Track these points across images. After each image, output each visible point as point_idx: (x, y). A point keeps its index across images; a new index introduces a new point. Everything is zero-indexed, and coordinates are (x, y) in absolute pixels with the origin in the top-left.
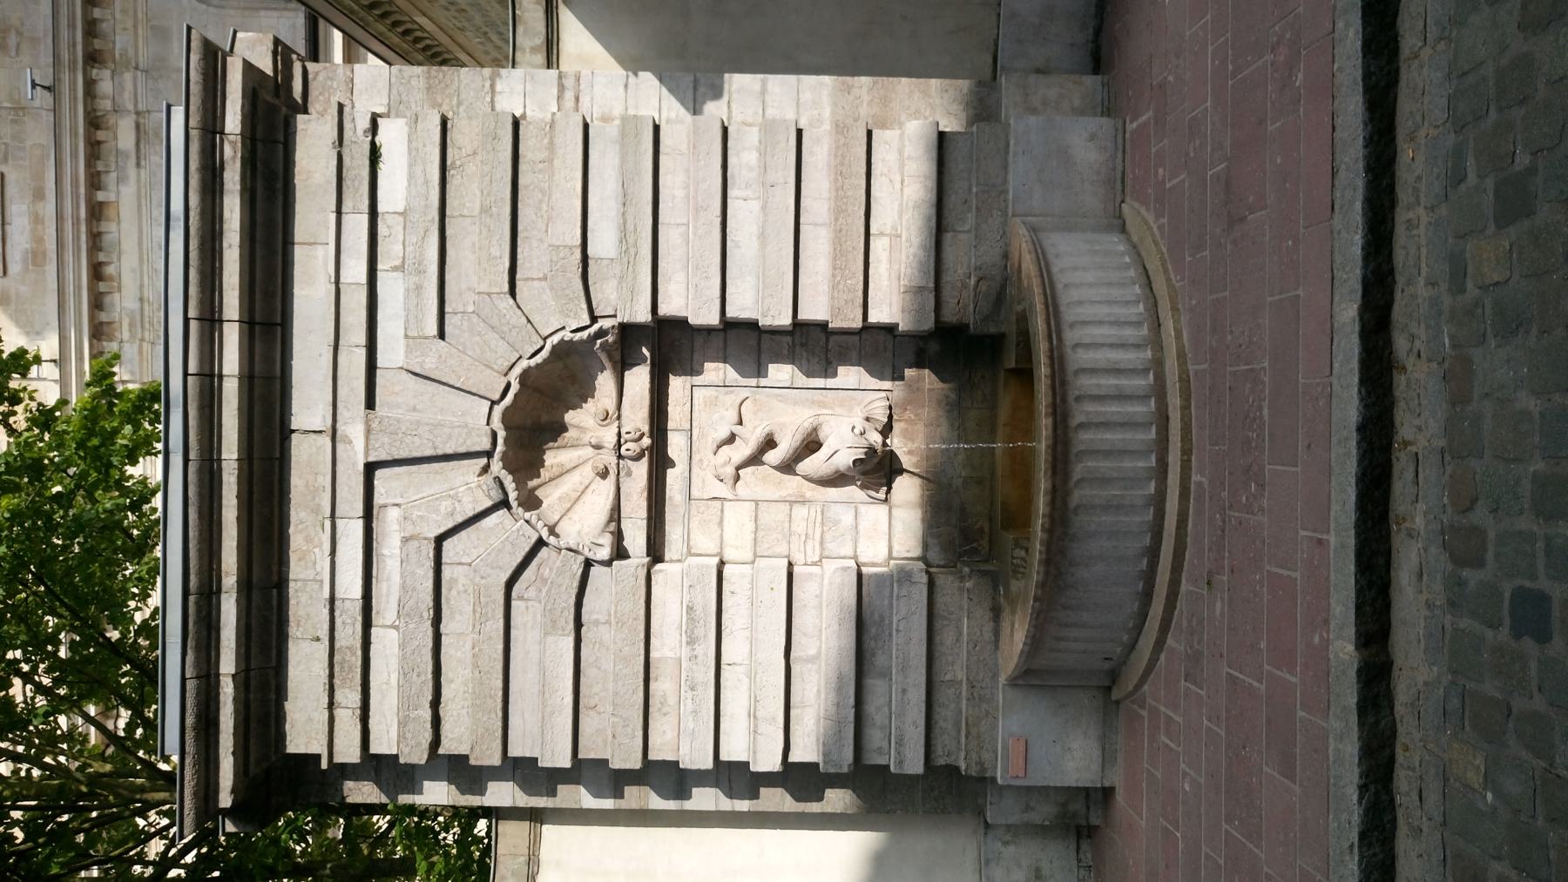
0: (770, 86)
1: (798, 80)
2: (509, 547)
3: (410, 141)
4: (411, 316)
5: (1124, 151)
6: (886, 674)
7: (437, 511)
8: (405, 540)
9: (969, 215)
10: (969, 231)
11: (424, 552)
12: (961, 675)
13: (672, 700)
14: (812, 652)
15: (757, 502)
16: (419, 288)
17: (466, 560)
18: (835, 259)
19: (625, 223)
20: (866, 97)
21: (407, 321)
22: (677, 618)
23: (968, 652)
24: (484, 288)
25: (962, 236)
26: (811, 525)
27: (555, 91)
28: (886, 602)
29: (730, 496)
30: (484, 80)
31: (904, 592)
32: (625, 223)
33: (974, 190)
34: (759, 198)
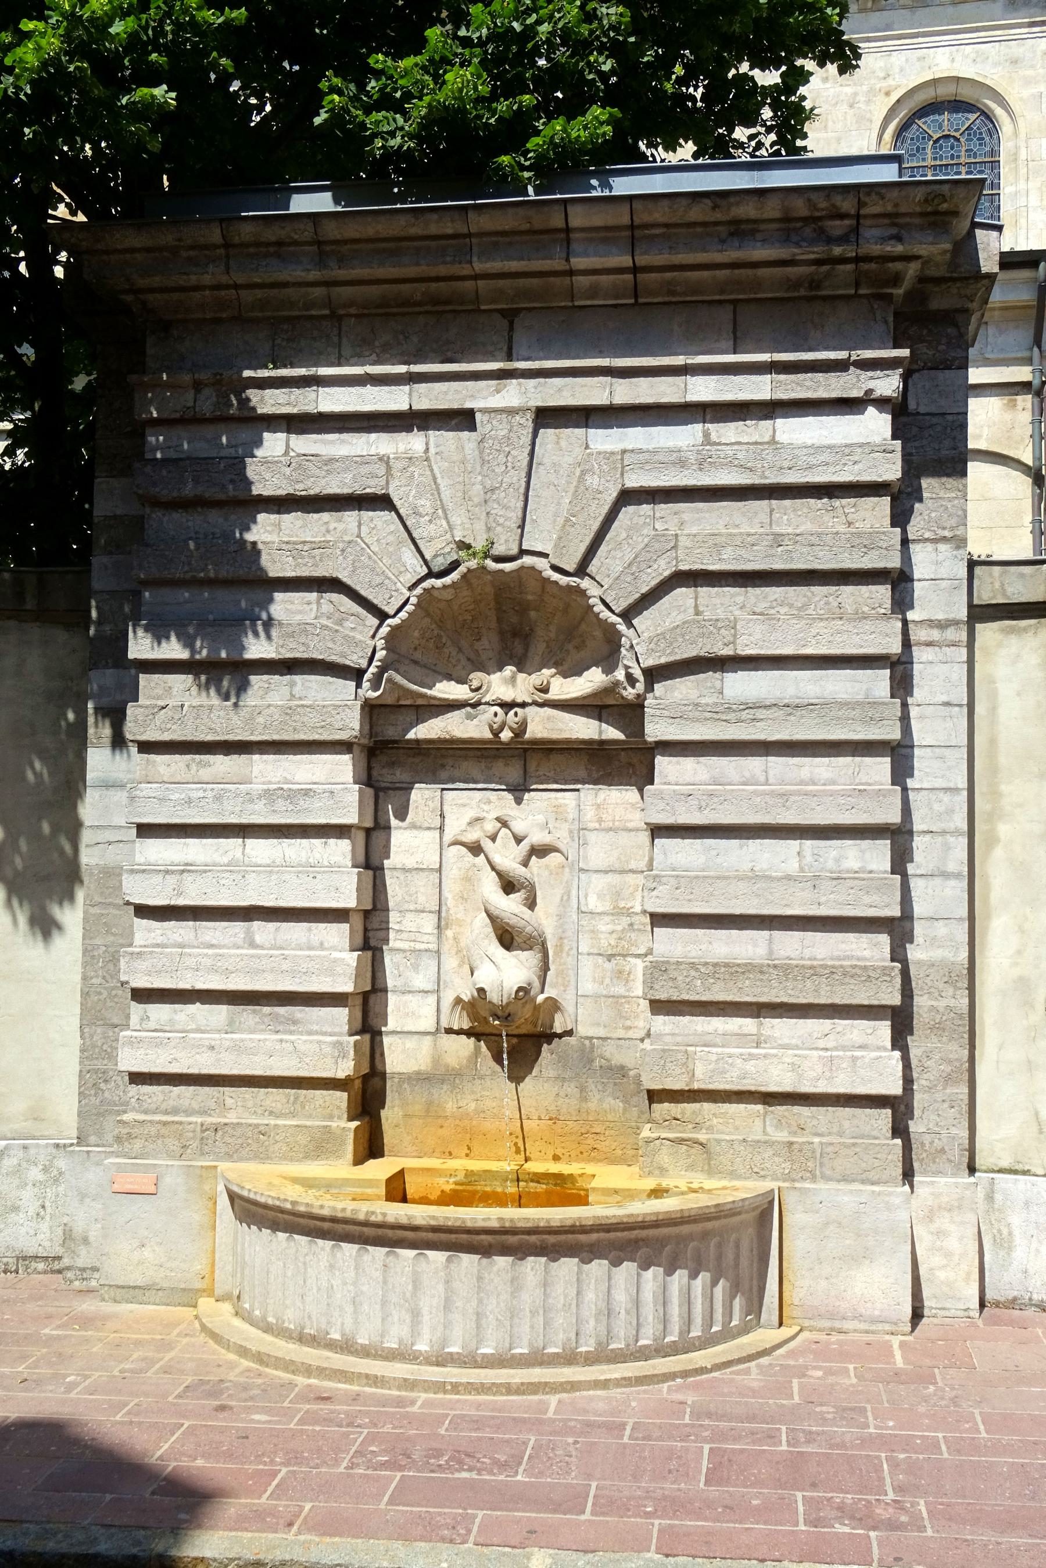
0: (953, 883)
1: (961, 919)
2: (378, 580)
3: (861, 445)
4: (651, 458)
5: (867, 1332)
6: (231, 1027)
7: (419, 495)
8: (385, 460)
9: (786, 1134)
10: (765, 1133)
11: (372, 482)
12: (232, 1118)
13: (205, 774)
14: (258, 939)
15: (440, 870)
16: (682, 463)
17: (364, 529)
18: (727, 965)
19: (766, 707)
20: (941, 1004)
21: (641, 451)
22: (297, 778)
23: (257, 1126)
24: (683, 541)
25: (758, 1123)
26: (412, 936)
27: (941, 616)
28: (315, 1027)
29: (448, 838)
30: (952, 529)
31: (327, 1050)
32: (766, 707)
33: (816, 1140)
34: (802, 870)
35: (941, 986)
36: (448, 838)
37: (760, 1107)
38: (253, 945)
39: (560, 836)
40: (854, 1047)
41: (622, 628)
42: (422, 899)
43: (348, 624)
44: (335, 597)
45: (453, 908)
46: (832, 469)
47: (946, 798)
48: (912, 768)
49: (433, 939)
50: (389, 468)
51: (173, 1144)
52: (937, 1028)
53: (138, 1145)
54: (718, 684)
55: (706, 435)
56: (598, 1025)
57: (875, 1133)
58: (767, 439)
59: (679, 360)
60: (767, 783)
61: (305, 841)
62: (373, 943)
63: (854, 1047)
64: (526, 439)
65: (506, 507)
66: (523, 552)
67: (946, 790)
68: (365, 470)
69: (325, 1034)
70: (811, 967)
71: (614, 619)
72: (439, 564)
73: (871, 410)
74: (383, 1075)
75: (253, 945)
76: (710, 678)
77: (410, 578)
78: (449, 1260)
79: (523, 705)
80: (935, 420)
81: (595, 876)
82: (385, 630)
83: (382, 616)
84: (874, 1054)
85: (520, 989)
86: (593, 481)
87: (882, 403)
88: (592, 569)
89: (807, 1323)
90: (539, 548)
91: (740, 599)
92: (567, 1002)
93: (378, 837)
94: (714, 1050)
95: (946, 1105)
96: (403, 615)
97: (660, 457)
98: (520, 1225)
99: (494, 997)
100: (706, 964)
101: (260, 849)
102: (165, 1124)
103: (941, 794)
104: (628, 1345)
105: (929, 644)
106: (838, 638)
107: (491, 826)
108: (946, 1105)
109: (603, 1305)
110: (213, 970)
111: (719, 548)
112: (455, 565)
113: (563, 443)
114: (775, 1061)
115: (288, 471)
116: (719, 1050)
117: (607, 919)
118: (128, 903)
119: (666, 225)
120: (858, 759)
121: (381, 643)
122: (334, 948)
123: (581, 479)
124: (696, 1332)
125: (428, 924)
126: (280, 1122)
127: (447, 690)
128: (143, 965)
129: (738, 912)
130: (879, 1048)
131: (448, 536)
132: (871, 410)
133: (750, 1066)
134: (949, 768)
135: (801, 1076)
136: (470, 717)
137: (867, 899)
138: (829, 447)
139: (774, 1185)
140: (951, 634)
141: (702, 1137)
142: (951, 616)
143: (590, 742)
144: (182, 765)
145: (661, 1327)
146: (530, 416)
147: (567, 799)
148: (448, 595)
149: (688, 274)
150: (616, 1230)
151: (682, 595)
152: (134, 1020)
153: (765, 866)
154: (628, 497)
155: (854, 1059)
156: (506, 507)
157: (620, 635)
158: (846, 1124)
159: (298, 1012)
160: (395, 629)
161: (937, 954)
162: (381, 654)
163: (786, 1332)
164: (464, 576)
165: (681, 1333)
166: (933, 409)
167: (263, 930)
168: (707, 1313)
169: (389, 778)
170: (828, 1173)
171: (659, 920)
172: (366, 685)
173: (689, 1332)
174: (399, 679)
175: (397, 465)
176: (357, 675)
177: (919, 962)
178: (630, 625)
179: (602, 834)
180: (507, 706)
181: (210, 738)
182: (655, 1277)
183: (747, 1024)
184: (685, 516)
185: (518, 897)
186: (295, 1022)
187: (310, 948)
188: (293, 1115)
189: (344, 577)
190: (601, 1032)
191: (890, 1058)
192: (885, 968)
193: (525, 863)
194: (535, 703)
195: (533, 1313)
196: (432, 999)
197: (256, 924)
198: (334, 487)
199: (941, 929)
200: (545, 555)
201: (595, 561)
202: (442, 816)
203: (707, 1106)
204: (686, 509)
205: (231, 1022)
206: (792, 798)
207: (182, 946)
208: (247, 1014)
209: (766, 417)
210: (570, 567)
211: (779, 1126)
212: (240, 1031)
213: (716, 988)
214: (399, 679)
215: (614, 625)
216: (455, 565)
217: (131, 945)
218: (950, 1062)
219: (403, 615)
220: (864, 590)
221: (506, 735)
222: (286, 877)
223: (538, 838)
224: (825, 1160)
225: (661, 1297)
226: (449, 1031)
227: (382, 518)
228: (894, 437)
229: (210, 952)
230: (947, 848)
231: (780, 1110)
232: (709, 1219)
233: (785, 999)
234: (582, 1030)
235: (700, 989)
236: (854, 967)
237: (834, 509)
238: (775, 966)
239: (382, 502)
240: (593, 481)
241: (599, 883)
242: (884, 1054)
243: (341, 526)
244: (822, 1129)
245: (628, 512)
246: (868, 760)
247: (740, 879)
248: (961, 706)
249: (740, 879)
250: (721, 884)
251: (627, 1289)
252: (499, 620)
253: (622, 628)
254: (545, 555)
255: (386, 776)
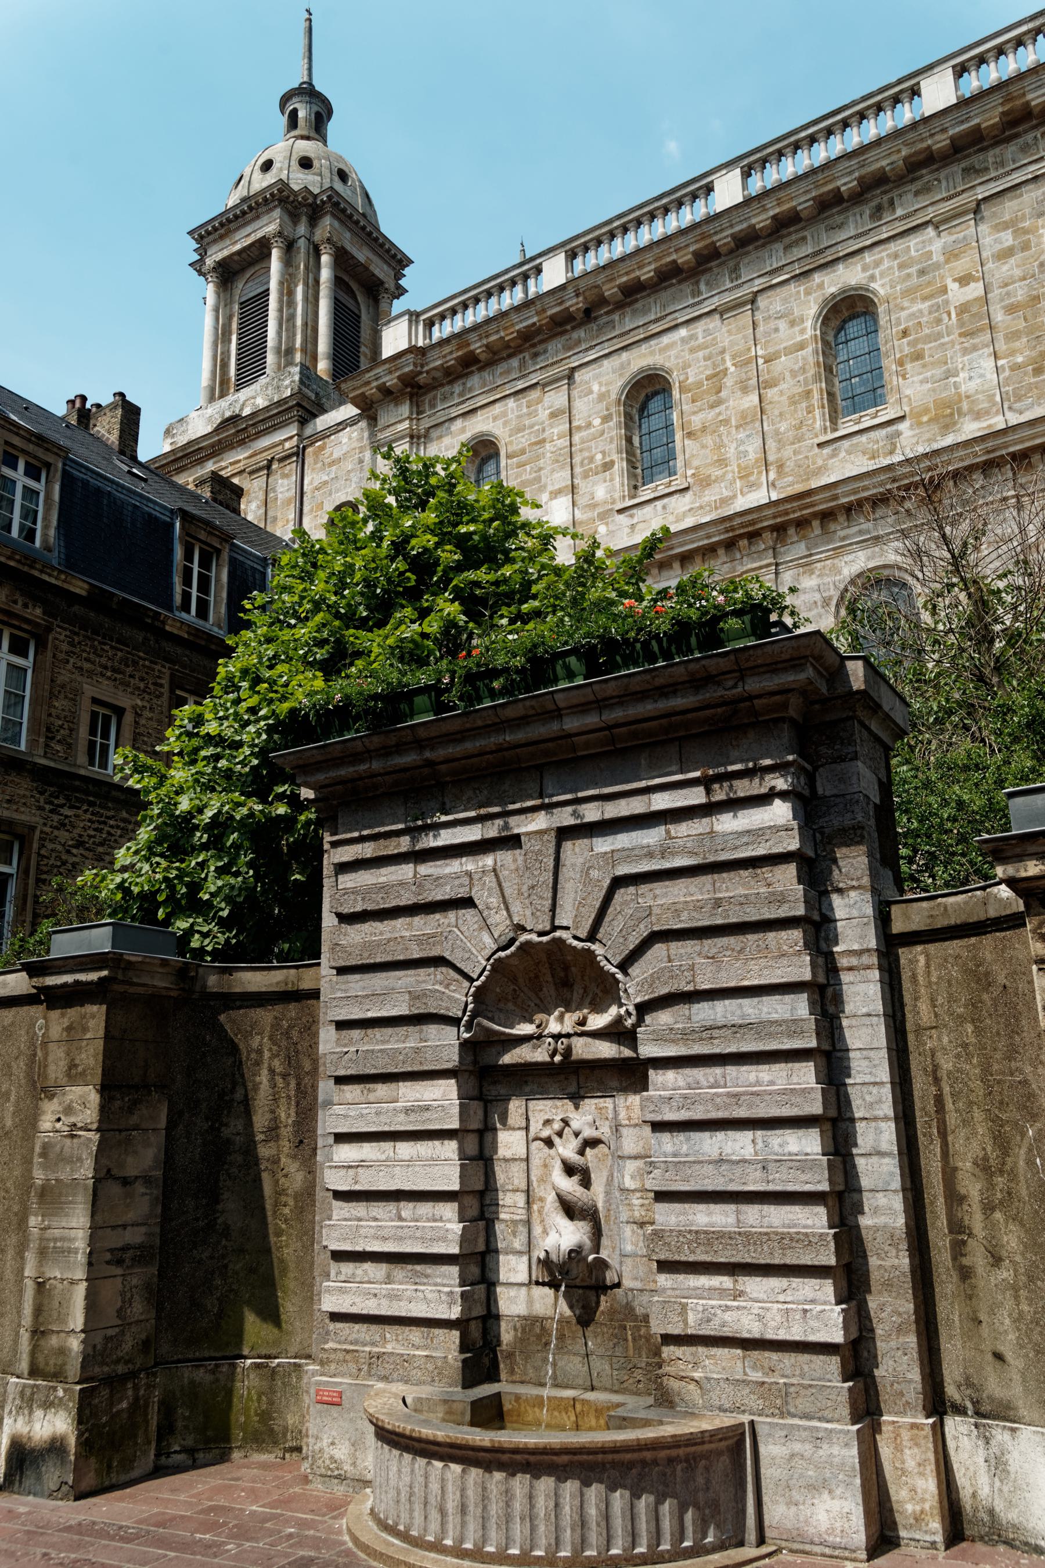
0: (886, 1160)
2: (467, 955)
3: (770, 827)
4: (628, 855)
5: (831, 1557)
6: (389, 1279)
7: (490, 896)
8: (469, 874)
9: (760, 1374)
10: (745, 1374)
11: (462, 890)
12: (389, 1348)
13: (372, 1097)
14: (403, 1214)
15: (527, 1159)
16: (650, 855)
17: (460, 922)
18: (706, 1232)
19: (719, 1028)
20: (887, 1263)
21: (624, 850)
22: (425, 1097)
23: (402, 1355)
24: (656, 911)
25: (739, 1364)
26: (512, 1210)
27: (856, 947)
28: (439, 1280)
29: (532, 1135)
30: (858, 879)
31: (444, 1297)
32: (719, 1028)
33: (782, 1381)
34: (756, 1154)
35: (887, 1248)
36: (532, 1135)
37: (739, 1351)
38: (400, 1219)
39: (604, 1131)
40: (806, 1302)
41: (620, 976)
42: (516, 1182)
43: (452, 987)
44: (444, 969)
45: (538, 1190)
46: (751, 847)
47: (874, 1090)
48: (849, 1068)
49: (524, 1211)
50: (471, 879)
51: (353, 1367)
52: (888, 1285)
53: (333, 1366)
54: (687, 1013)
55: (668, 832)
56: (636, 1279)
57: (828, 1376)
58: (708, 830)
59: (643, 784)
60: (725, 1086)
61: (430, 1143)
62: (487, 1215)
63: (806, 1302)
64: (552, 850)
65: (541, 898)
66: (554, 928)
67: (875, 1084)
68: (457, 882)
69: (444, 1285)
70: (766, 1234)
71: (614, 970)
72: (504, 940)
73: (777, 802)
74: (497, 1317)
75: (400, 1219)
76: (682, 1009)
77: (487, 952)
78: (463, 1471)
79: (568, 1036)
80: (838, 800)
81: (628, 1162)
82: (473, 989)
83: (471, 980)
84: (819, 1308)
85: (571, 1251)
86: (595, 874)
87: (783, 795)
88: (599, 936)
89: (784, 1544)
90: (565, 924)
91: (698, 948)
92: (613, 1261)
93: (488, 1137)
94: (701, 1302)
95: (900, 1353)
96: (483, 978)
97: (636, 852)
98: (506, 1445)
99: (554, 1257)
100: (690, 1231)
101: (405, 1149)
102: (347, 1351)
103: (871, 1087)
104: (599, 1553)
105: (850, 969)
106: (765, 972)
107: (557, 1126)
108: (900, 1353)
109: (577, 1517)
110: (376, 1238)
111: (677, 913)
112: (512, 941)
113: (577, 850)
114: (745, 1312)
115: (414, 888)
116: (704, 1302)
117: (638, 1195)
118: (328, 1190)
119: (618, 697)
120: (790, 1065)
121: (470, 999)
122: (449, 1221)
123: (587, 874)
124: (665, 1546)
125: (520, 1199)
126: (417, 1353)
127: (526, 1029)
128: (335, 1234)
129: (710, 1188)
130: (825, 1303)
131: (508, 922)
132: (777, 802)
133: (728, 1316)
134: (875, 1066)
135: (765, 1325)
136: (536, 1047)
137: (804, 1177)
138: (748, 832)
139: (745, 1418)
140: (866, 959)
141: (697, 1375)
142: (865, 946)
143: (613, 1060)
144: (359, 1091)
145: (630, 1539)
146: (553, 834)
147: (608, 1103)
148: (515, 962)
149: (645, 725)
150: (581, 1453)
151: (659, 950)
152: (333, 1274)
153: (730, 1151)
154: (619, 882)
155: (805, 1311)
156: (541, 898)
157: (617, 981)
158: (806, 1368)
159: (429, 1269)
160: (478, 988)
161: (881, 1220)
162: (470, 1007)
163: (764, 1550)
164: (520, 948)
165: (574, 1551)
166: (835, 792)
167: (407, 1209)
168: (653, 1530)
169: (494, 1093)
170: (792, 1410)
171: (662, 1196)
172: (462, 1029)
173: (658, 1545)
174: (486, 1023)
175: (476, 877)
176: (455, 1022)
177: (867, 1228)
178: (626, 974)
179: (631, 1129)
180: (557, 1037)
181: (373, 1071)
182: (622, 1496)
183: (725, 1281)
184: (658, 892)
185: (576, 1178)
186: (427, 1276)
187: (435, 1220)
188: (426, 1347)
189: (447, 955)
190: (638, 1285)
191: (832, 1310)
192: (821, 1235)
193: (581, 1152)
194: (576, 1034)
195: (522, 1519)
196: (525, 1258)
197: (402, 1204)
198: (439, 895)
199: (881, 1200)
200: (567, 928)
201: (602, 930)
202: (527, 1119)
203: (701, 1350)
204: (659, 888)
205: (388, 1276)
206: (743, 1098)
207: (360, 1220)
208: (400, 1272)
209: (705, 816)
210: (583, 935)
211: (754, 1368)
212: (394, 1282)
213: (698, 1251)
214: (486, 1023)
215: (613, 975)
216: (512, 941)
217: (330, 1219)
218: (900, 1314)
219: (483, 978)
220: (783, 934)
221: (558, 1058)
222: (417, 1169)
223: (588, 1133)
224: (790, 1399)
225: (628, 1513)
226: (537, 1283)
227: (468, 914)
228: (794, 819)
229: (374, 1224)
230: (879, 1132)
231: (755, 1354)
232: (696, 1444)
233: (749, 1260)
234: (627, 1283)
235: (687, 1252)
236: (798, 1233)
237: (757, 875)
238: (740, 1233)
239: (467, 902)
240: (595, 874)
241: (631, 1166)
242: (827, 1307)
243: (446, 921)
244: (788, 1372)
245: (623, 895)
246: (797, 1065)
247: (710, 1162)
248: (878, 1015)
249: (710, 1162)
250: (698, 1167)
251: (597, 1505)
252: (553, 976)
253: (620, 976)
254: (567, 928)
255: (494, 1091)
